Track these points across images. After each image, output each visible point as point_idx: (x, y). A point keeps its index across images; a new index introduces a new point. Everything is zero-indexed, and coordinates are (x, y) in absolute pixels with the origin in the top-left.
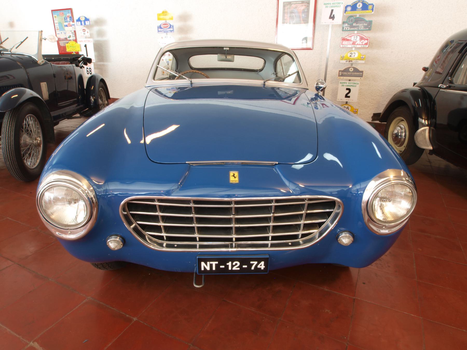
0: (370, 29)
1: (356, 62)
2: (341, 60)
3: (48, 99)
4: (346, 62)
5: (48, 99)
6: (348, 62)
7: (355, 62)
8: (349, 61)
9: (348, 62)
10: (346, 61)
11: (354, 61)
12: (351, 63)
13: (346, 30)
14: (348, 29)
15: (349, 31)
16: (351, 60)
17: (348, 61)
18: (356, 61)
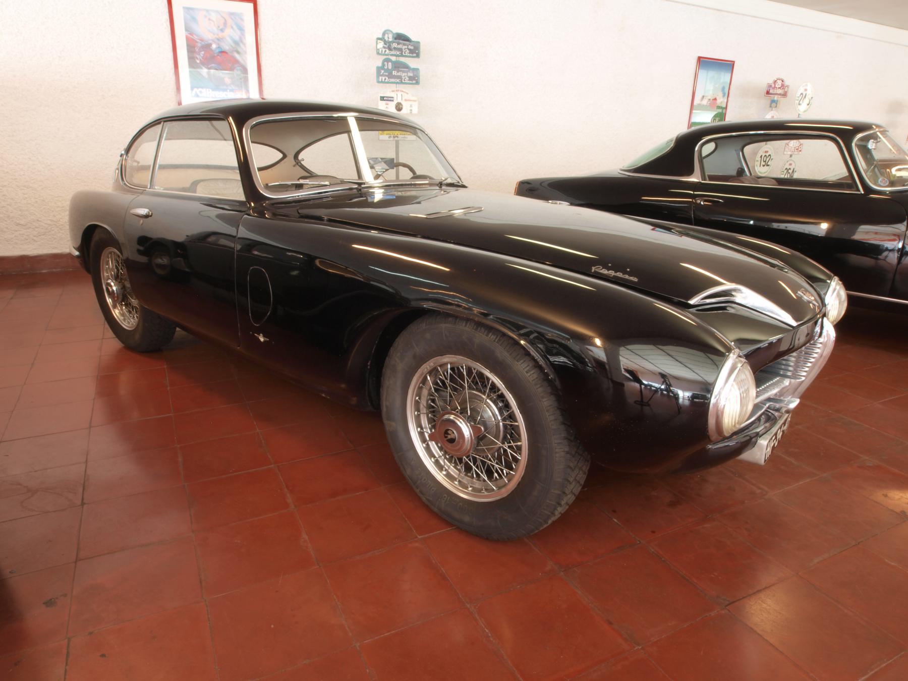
0: (417, 83)
1: (404, 137)
2: (381, 134)
3: (762, 462)
4: (390, 137)
5: (762, 462)
6: (392, 139)
7: (403, 139)
8: (394, 137)
9: (392, 139)
10: (388, 136)
11: (401, 136)
12: (396, 141)
13: (383, 80)
14: (386, 81)
15: (388, 83)
16: (396, 135)
17: (392, 136)
18: (403, 136)
